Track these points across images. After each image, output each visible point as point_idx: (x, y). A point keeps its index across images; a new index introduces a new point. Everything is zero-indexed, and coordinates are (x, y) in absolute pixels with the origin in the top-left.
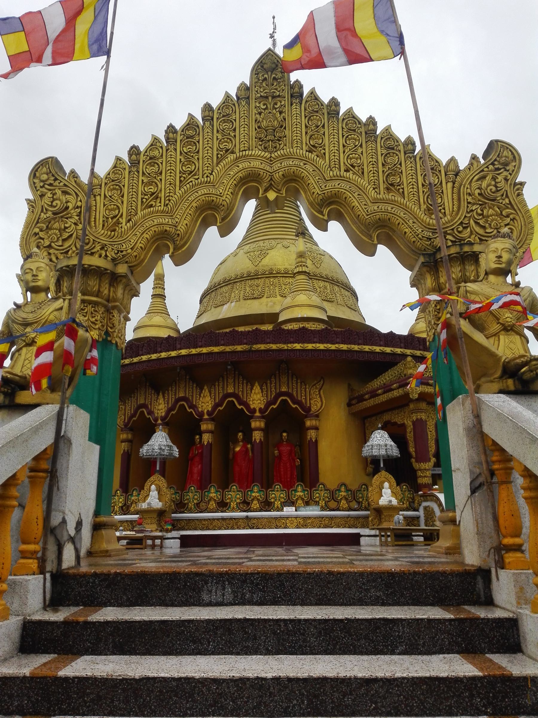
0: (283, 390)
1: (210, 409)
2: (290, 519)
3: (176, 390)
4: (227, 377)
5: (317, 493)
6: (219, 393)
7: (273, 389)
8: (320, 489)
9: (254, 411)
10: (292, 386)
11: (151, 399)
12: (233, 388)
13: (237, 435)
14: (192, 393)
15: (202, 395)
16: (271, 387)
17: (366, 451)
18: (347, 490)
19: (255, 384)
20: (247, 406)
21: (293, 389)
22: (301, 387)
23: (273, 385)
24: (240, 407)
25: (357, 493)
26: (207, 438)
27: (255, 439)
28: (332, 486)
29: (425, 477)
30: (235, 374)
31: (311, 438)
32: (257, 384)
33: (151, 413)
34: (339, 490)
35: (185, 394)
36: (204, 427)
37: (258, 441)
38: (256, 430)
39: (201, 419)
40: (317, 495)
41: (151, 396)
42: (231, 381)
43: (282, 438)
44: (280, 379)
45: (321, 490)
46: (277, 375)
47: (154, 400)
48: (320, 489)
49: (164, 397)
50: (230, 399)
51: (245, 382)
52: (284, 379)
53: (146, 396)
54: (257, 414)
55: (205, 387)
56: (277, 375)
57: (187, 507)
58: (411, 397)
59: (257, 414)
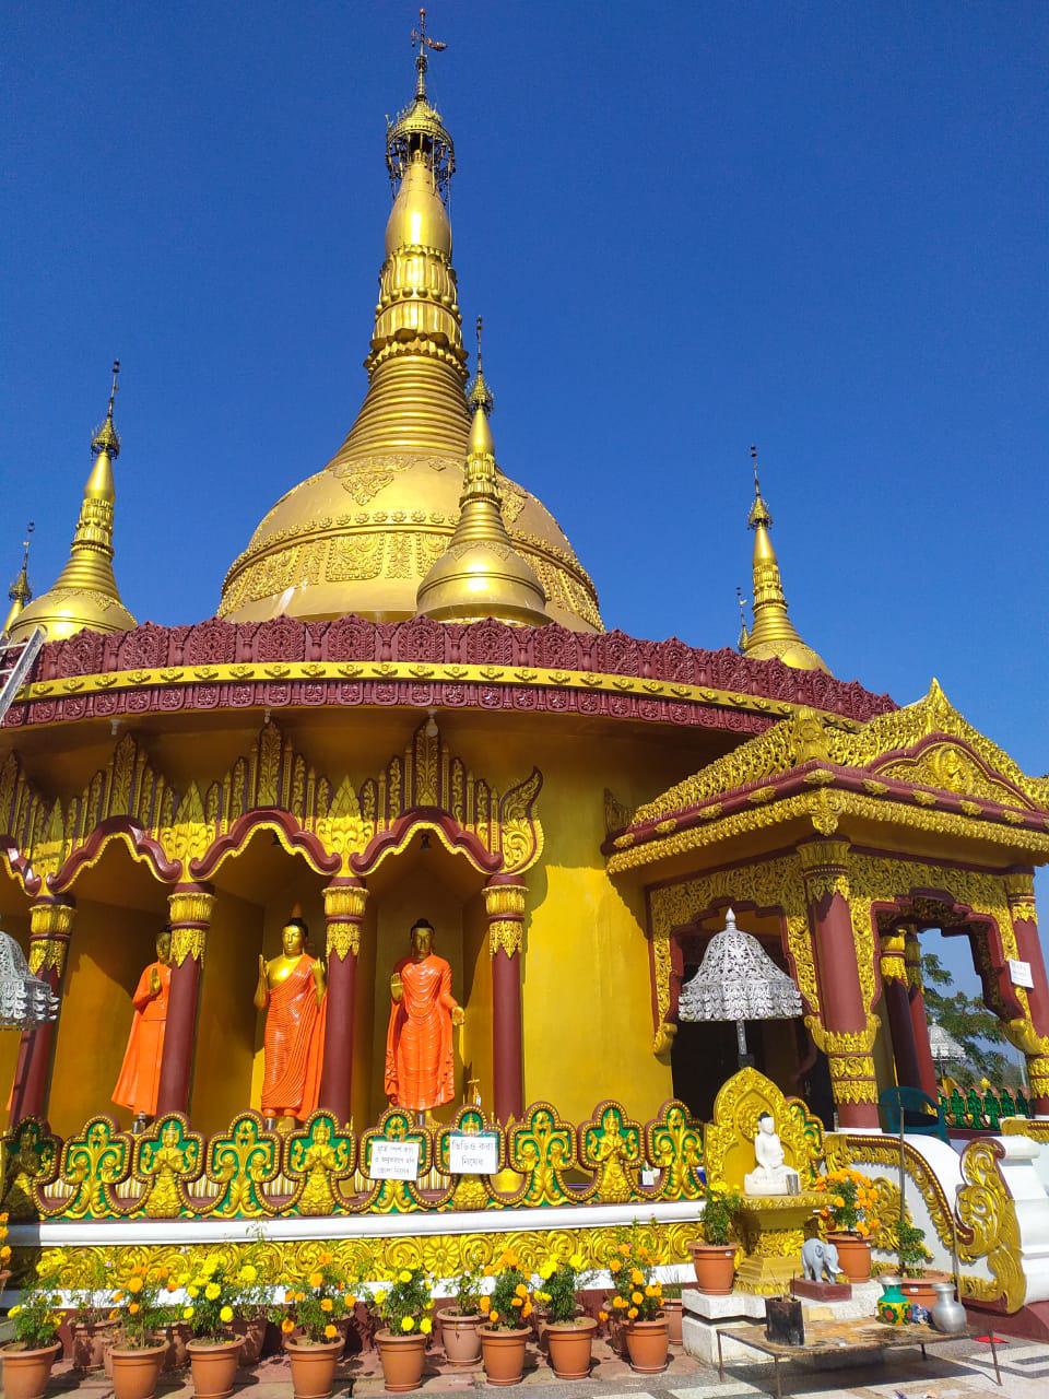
0: (423, 803)
1: (201, 856)
2: (435, 1242)
3: (102, 797)
4: (259, 761)
5: (527, 1141)
6: (231, 806)
7: (395, 800)
8: (537, 1126)
10: (451, 791)
12: (275, 794)
13: (281, 936)
14: (152, 805)
15: (180, 813)
16: (388, 791)
17: (698, 1005)
18: (624, 1129)
19: (342, 780)
20: (315, 847)
21: (451, 798)
22: (476, 797)
23: (396, 781)
24: (292, 850)
25: (654, 1136)
26: (185, 944)
28: (576, 1117)
29: (860, 1078)
30: (282, 752)
31: (501, 947)
32: (347, 783)
34: (599, 1130)
35: (131, 810)
36: (178, 910)
37: (342, 954)
38: (338, 921)
39: (172, 888)
40: (529, 1148)
42: (270, 770)
43: (414, 944)
44: (415, 770)
45: (542, 1131)
46: (409, 758)
47: (36, 826)
48: (537, 1126)
49: (65, 815)
50: (265, 826)
51: (312, 776)
52: (428, 770)
53: (13, 814)
54: (345, 872)
55: (193, 790)
56: (409, 758)
57: (77, 1197)
58: (817, 825)
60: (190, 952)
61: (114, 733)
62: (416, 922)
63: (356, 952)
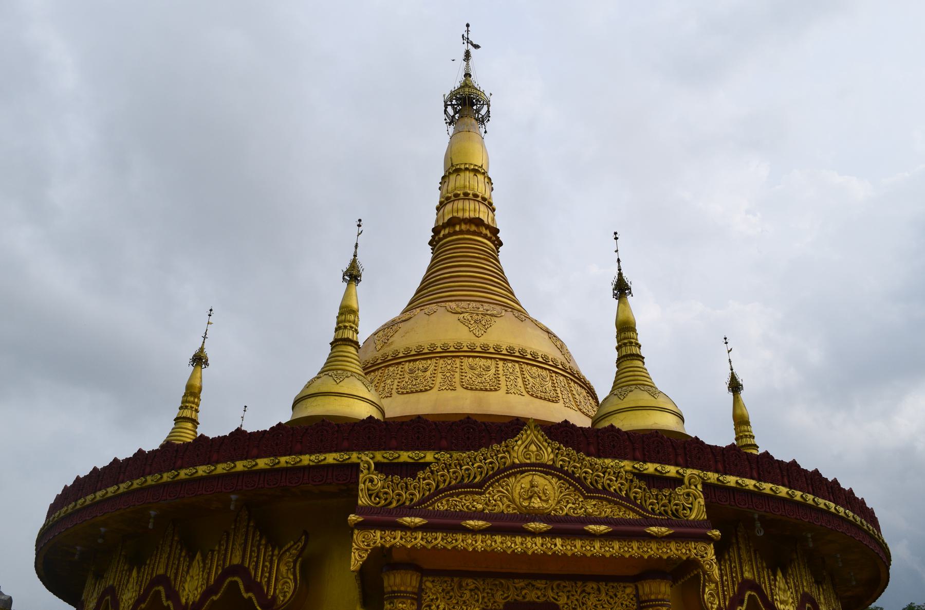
11: (177, 569)
33: (173, 595)
41: (179, 561)
61: (232, 507)
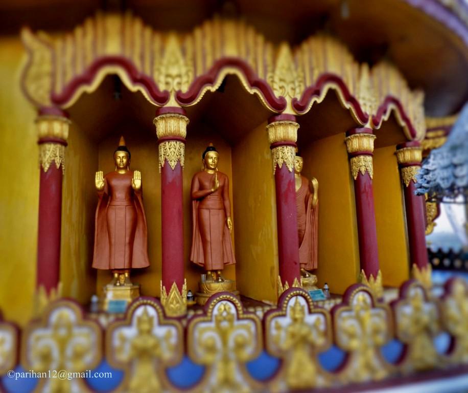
9: (163, 98)
20: (149, 84)
27: (166, 160)
37: (173, 164)
54: (172, 103)
59: (172, 103)
60: (54, 161)
62: (205, 150)
63: (182, 163)
